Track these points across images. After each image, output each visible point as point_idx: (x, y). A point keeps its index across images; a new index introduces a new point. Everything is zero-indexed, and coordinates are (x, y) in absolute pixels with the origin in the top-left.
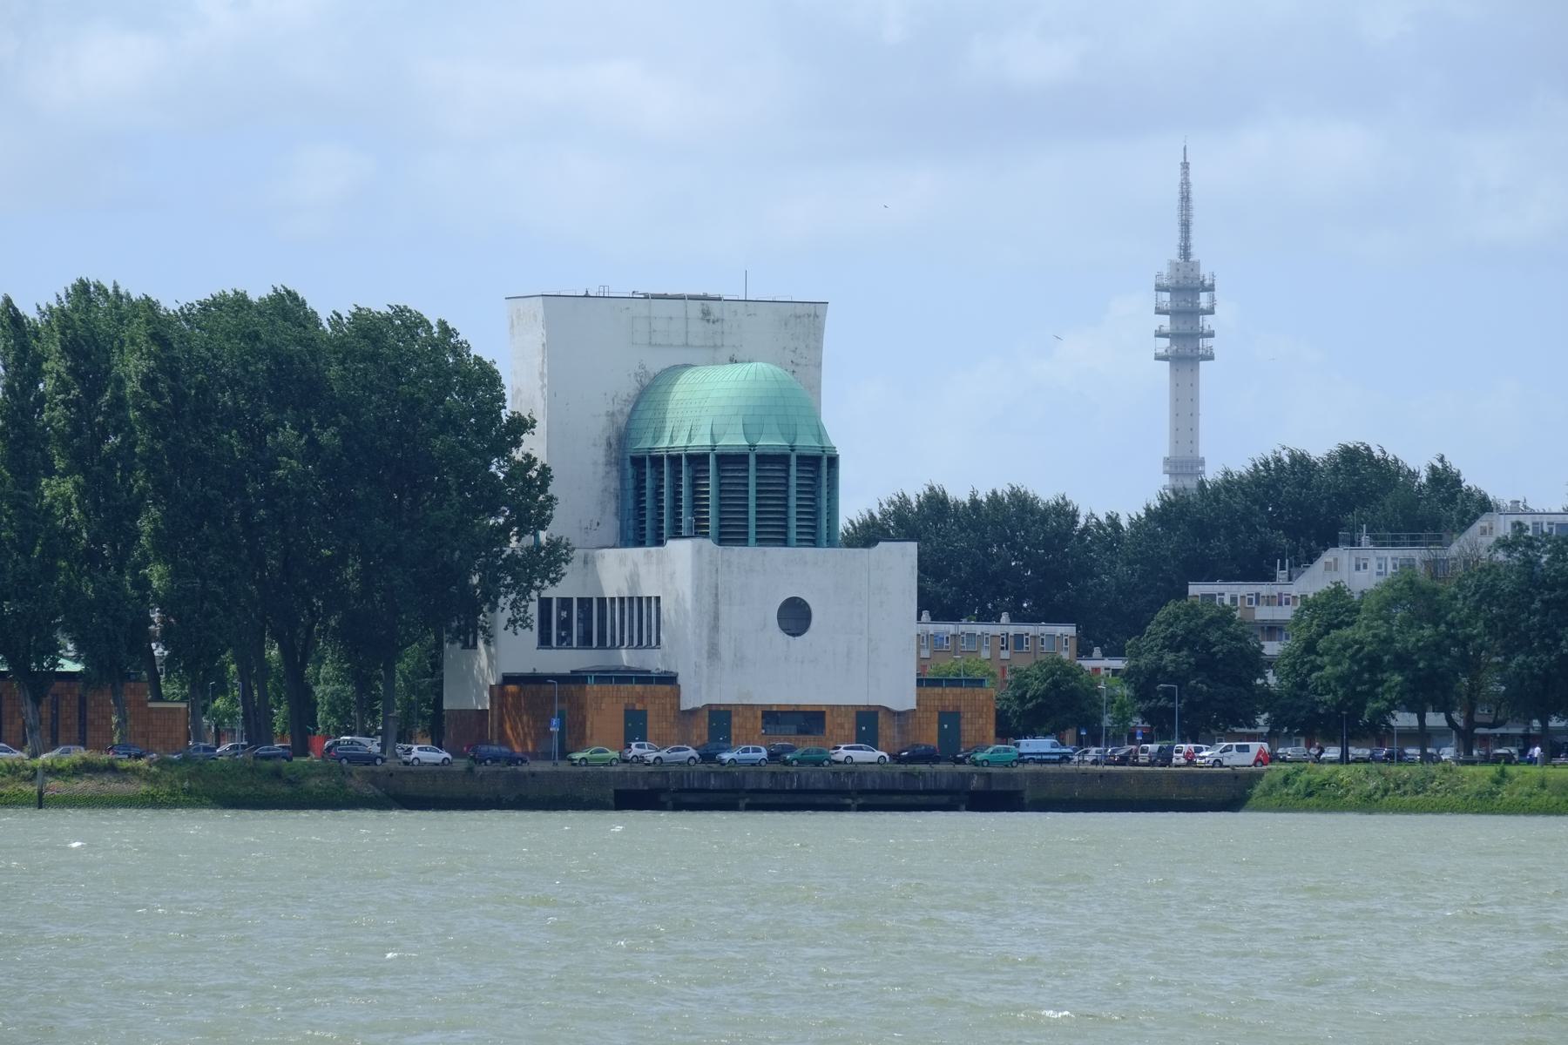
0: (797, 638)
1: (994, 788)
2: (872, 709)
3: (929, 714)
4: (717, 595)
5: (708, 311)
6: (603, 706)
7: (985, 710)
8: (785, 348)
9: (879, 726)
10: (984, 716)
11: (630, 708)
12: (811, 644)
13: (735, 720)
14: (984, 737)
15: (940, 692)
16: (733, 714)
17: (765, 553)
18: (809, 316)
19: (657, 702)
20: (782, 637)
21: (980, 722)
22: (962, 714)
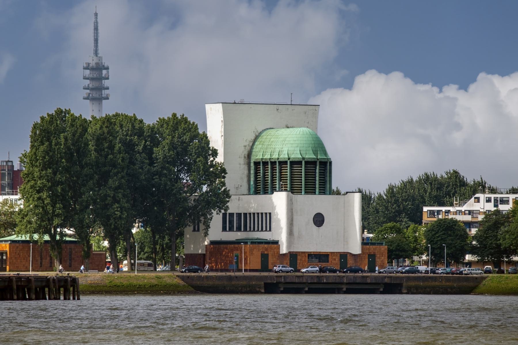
2: (346, 254)
4: (292, 212)
6: (254, 252)
11: (263, 253)
13: (299, 257)
21: (382, 258)
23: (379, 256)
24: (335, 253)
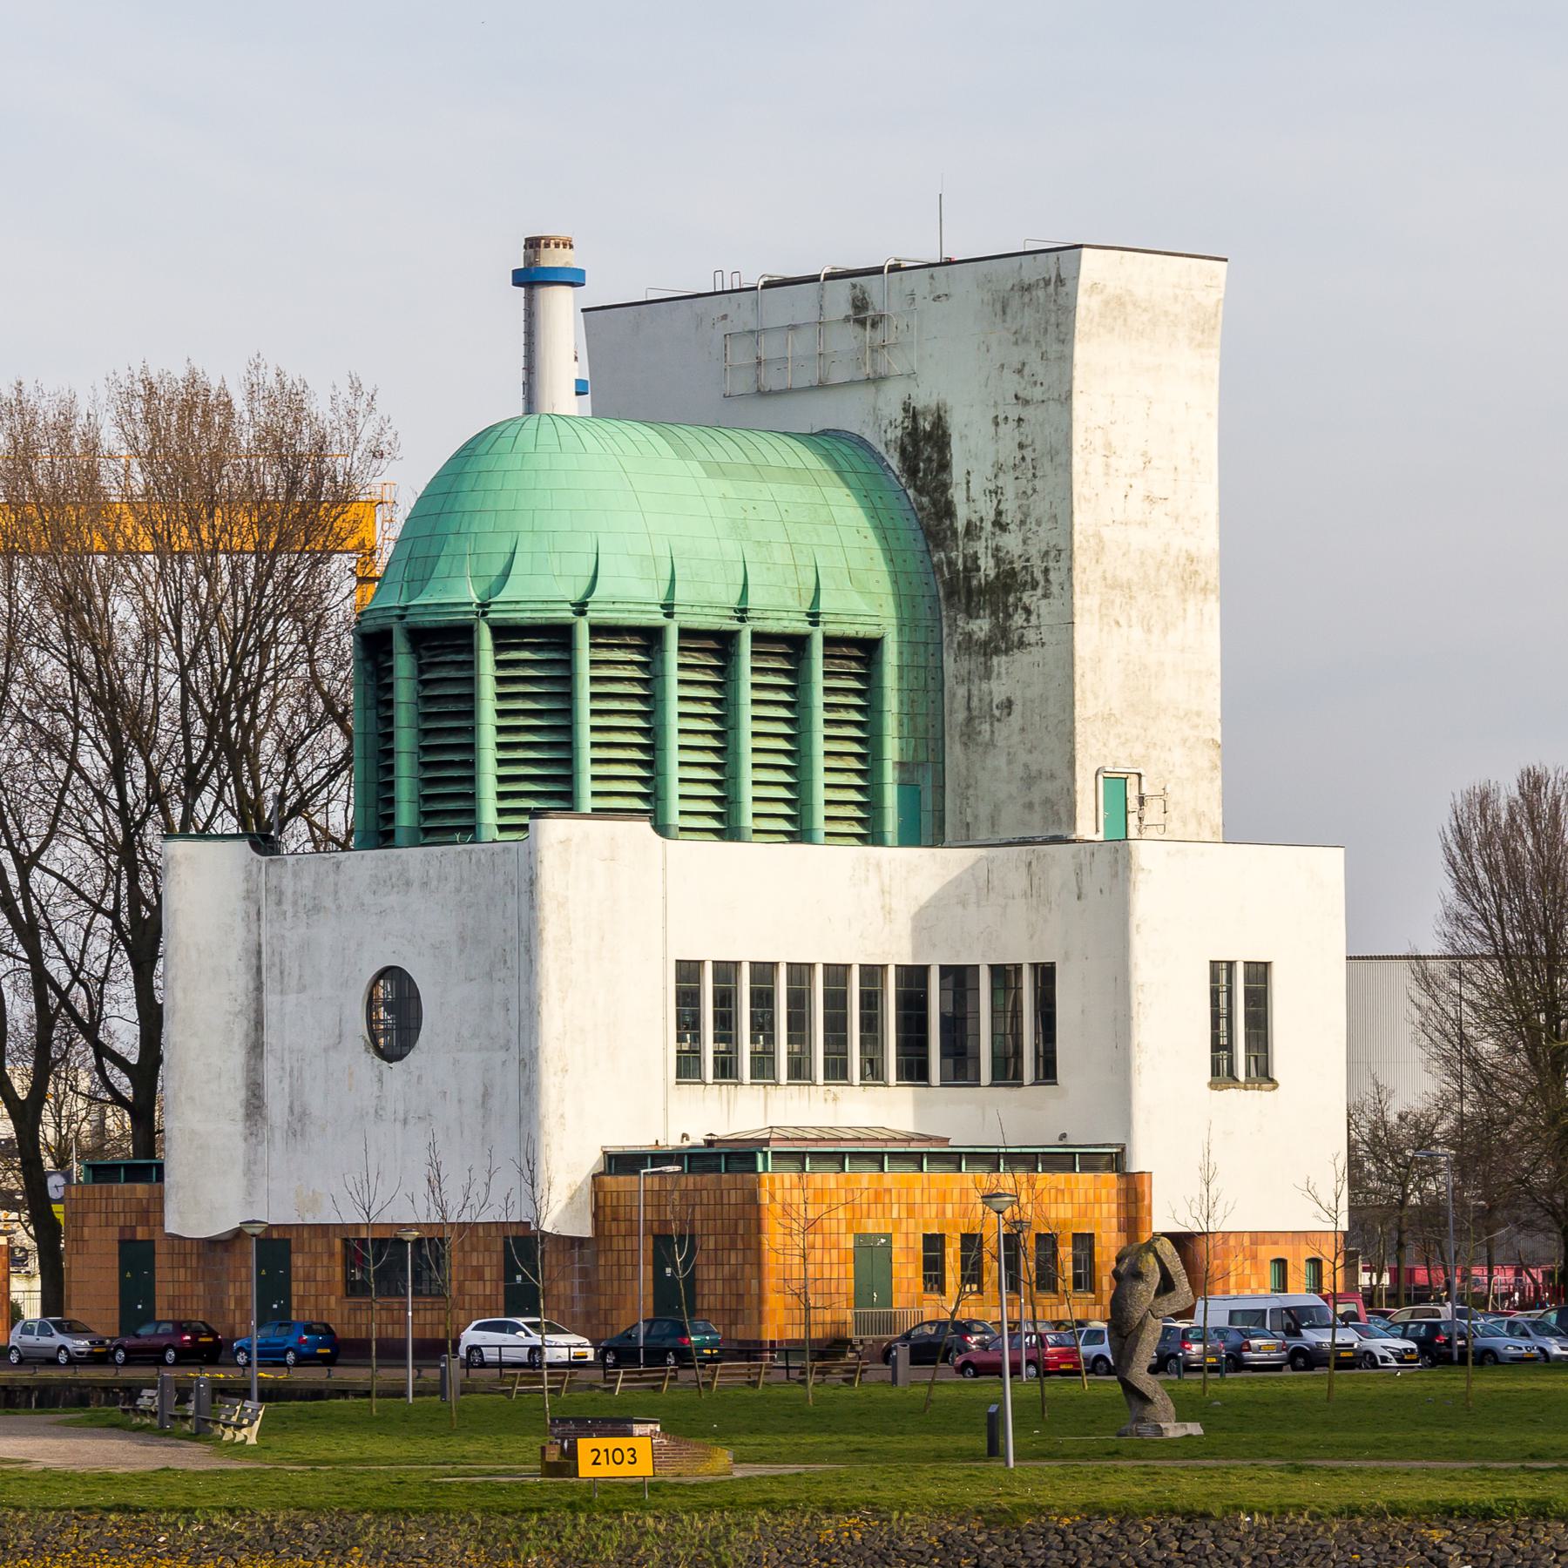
5: (864, 298)
7: (741, 1231)
10: (740, 1246)
11: (128, 1237)
12: (420, 1077)
14: (740, 1296)
17: (338, 865)
18: (1047, 283)
20: (368, 1063)
21: (733, 1261)
23: (712, 1246)
24: (493, 1229)
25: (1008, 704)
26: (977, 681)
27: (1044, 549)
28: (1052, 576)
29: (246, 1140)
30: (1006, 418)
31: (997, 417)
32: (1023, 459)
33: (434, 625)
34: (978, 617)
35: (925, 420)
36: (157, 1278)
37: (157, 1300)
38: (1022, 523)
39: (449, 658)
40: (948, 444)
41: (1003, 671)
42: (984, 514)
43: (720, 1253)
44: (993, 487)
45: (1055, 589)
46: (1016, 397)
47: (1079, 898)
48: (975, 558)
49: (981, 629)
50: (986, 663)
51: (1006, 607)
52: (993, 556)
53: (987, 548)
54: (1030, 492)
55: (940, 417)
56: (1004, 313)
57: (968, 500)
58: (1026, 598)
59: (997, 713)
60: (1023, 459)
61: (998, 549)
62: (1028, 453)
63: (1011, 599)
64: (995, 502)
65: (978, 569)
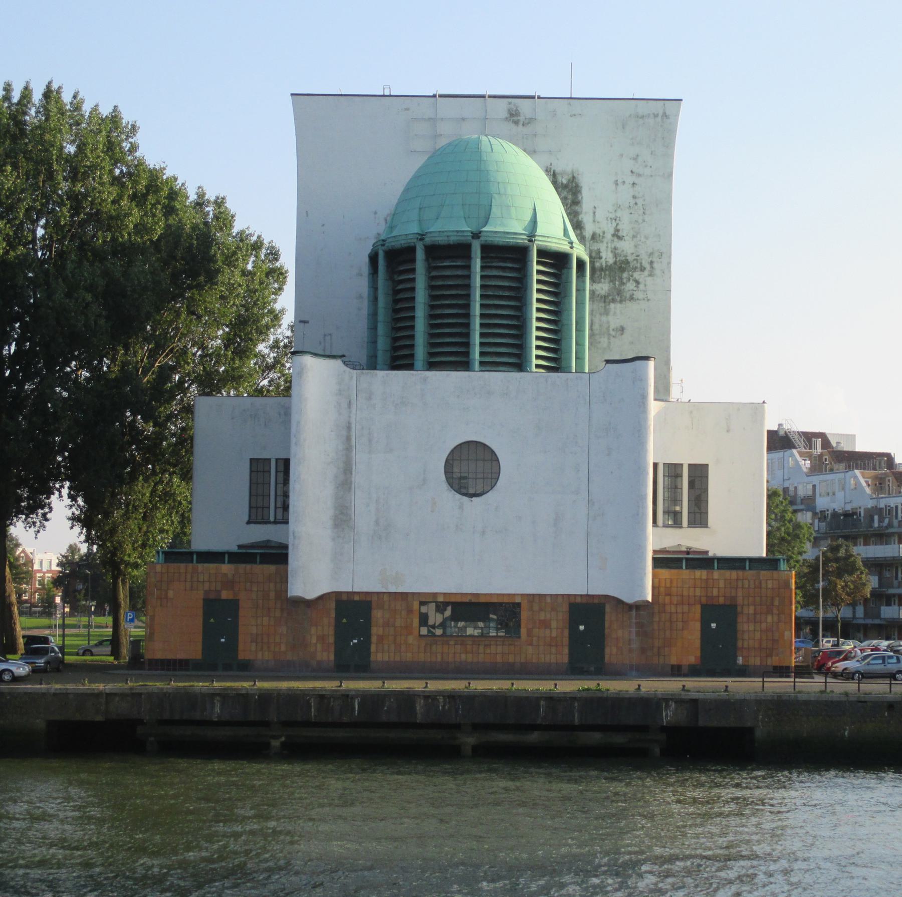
0: (474, 499)
1: (702, 722)
2: (596, 601)
3: (686, 608)
4: (348, 439)
5: (517, 110)
6: (171, 594)
7: (776, 603)
8: (622, 155)
9: (607, 625)
10: (775, 611)
11: (212, 596)
13: (377, 615)
15: (704, 577)
16: (374, 605)
17: (425, 379)
18: (656, 116)
19: (255, 589)
20: (450, 499)
21: (769, 619)
22: (739, 609)
23: (751, 611)
25: (622, 329)
26: (598, 316)
27: (650, 251)
28: (655, 265)
29: (333, 540)
30: (624, 182)
31: (617, 181)
32: (636, 204)
33: (505, 244)
34: (599, 282)
35: (562, 177)
36: (240, 623)
37: (241, 638)
38: (634, 237)
39: (495, 264)
40: (580, 192)
41: (618, 312)
42: (606, 229)
43: (758, 616)
44: (613, 216)
45: (658, 272)
46: (632, 172)
47: (728, 431)
48: (599, 252)
49: (602, 289)
50: (605, 307)
51: (621, 279)
52: (612, 252)
53: (607, 247)
54: (640, 221)
55: (574, 177)
56: (623, 127)
57: (594, 221)
58: (636, 275)
59: (613, 333)
60: (636, 204)
61: (615, 248)
62: (640, 202)
63: (625, 275)
64: (614, 224)
65: (600, 258)
